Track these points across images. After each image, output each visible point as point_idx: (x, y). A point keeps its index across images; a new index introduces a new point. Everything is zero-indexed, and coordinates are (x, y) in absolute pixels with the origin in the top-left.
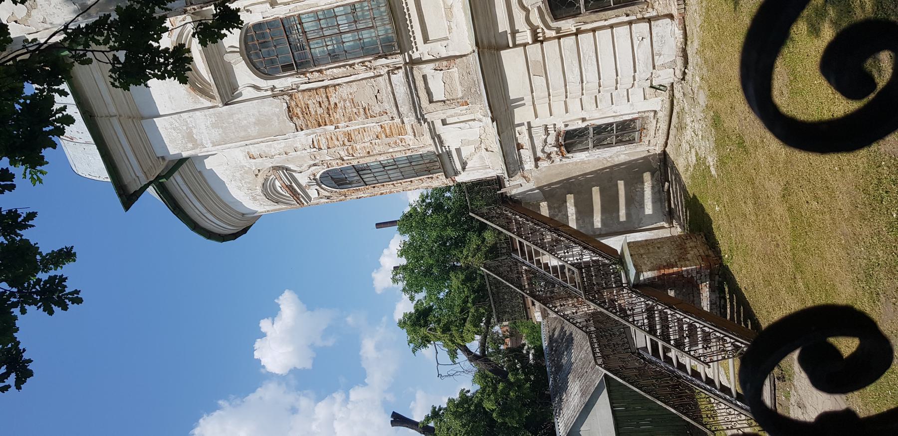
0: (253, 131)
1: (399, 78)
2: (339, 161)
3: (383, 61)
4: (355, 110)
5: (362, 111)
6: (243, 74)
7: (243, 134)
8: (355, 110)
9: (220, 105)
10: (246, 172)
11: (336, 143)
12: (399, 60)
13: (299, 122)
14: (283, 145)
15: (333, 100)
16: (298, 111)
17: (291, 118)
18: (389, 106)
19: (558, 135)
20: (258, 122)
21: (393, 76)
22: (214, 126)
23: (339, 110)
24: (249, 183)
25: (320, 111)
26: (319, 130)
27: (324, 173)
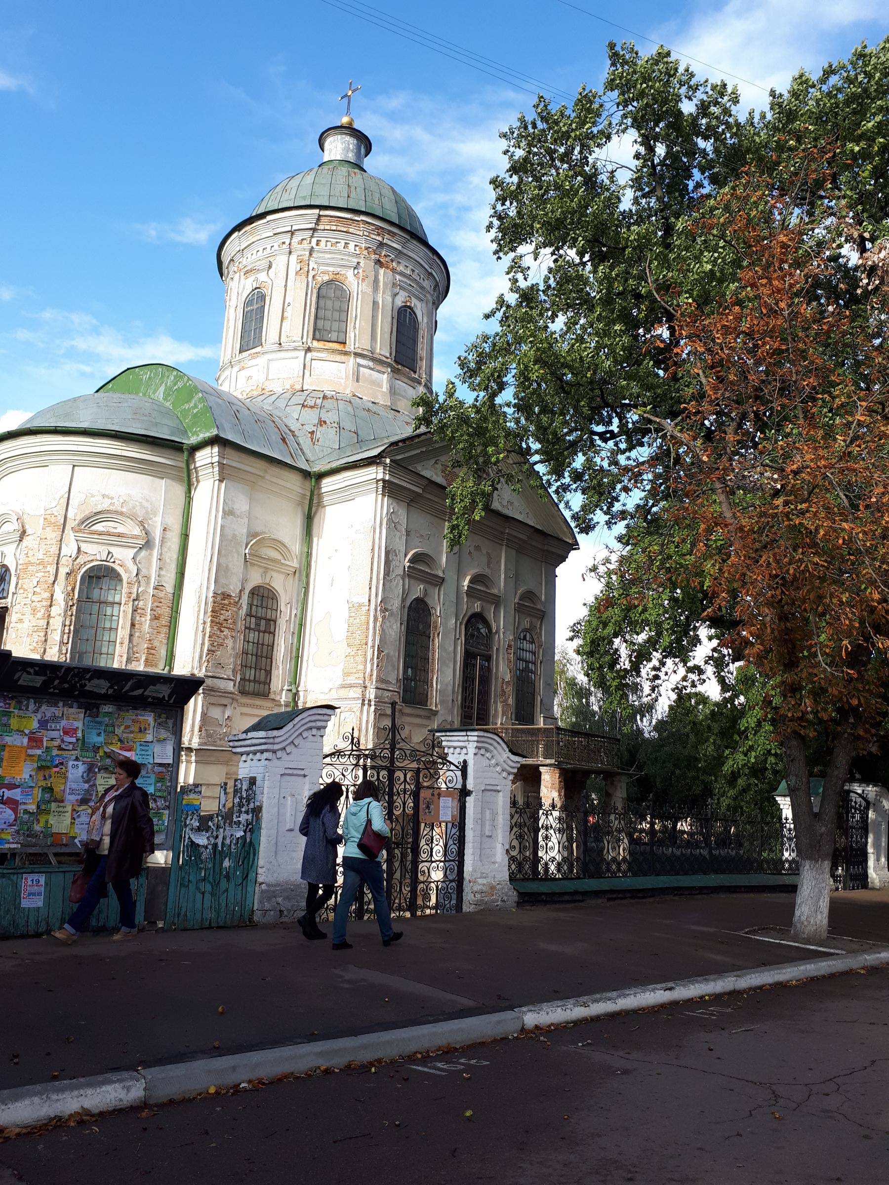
0: (223, 560)
1: (230, 686)
2: (134, 596)
4: (215, 644)
5: (213, 649)
6: (256, 579)
7: (223, 552)
8: (215, 644)
10: (147, 512)
11: (156, 604)
14: (168, 561)
15: (226, 631)
16: (226, 602)
17: (223, 594)
20: (227, 569)
21: (232, 683)
22: (234, 536)
24: (134, 508)
25: (222, 617)
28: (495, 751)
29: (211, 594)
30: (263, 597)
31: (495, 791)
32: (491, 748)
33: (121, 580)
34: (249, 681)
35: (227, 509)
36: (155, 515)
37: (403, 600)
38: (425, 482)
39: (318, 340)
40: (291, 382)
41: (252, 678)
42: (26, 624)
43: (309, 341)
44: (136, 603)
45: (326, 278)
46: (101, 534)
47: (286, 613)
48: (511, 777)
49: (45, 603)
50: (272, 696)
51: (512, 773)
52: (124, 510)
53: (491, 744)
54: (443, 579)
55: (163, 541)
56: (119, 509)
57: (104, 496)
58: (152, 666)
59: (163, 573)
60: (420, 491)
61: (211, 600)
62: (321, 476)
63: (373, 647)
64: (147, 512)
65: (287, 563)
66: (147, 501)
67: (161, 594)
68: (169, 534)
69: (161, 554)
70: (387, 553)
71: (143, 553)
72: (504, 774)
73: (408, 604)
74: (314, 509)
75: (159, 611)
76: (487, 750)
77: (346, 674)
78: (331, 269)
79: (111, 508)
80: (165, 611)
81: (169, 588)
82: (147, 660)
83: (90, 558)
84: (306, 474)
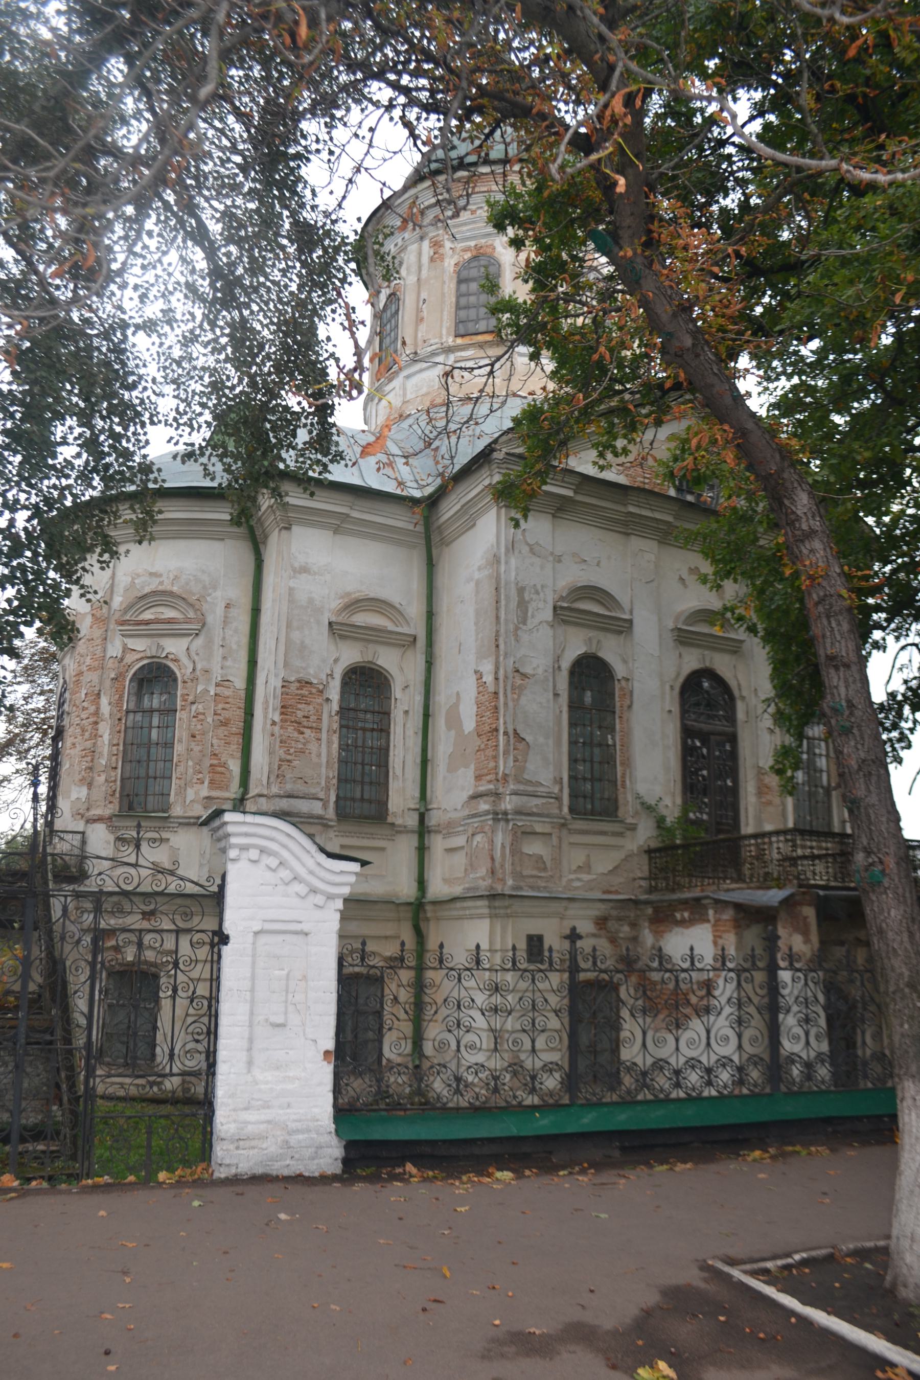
0: (296, 635)
1: (316, 808)
2: (191, 698)
3: (333, 798)
9: (333, 619)
10: (204, 587)
11: (220, 706)
12: (331, 813)
13: (293, 687)
14: (234, 647)
16: (304, 692)
17: (299, 681)
18: (289, 787)
19: (155, 965)
20: (303, 647)
21: (320, 804)
22: (311, 601)
23: (296, 734)
25: (300, 714)
26: (278, 703)
27: (173, 673)
28: (285, 854)
29: (280, 684)
30: (366, 682)
31: (296, 933)
32: (273, 846)
33: (175, 680)
34: (353, 799)
35: (297, 565)
36: (215, 588)
37: (558, 659)
38: (576, 480)
39: (462, 336)
40: (429, 398)
41: (358, 795)
42: (79, 748)
43: (451, 339)
44: (194, 707)
45: (468, 255)
46: (147, 623)
47: (405, 701)
48: (339, 904)
49: (92, 720)
50: (390, 819)
51: (337, 896)
52: (175, 589)
53: (272, 839)
54: (630, 622)
55: (226, 622)
56: (169, 588)
57: (151, 574)
58: (220, 788)
59: (229, 663)
60: (569, 493)
61: (279, 691)
62: (433, 502)
63: (506, 733)
64: (204, 587)
65: (399, 630)
66: (203, 572)
67: (227, 692)
68: (233, 612)
69: (224, 639)
70: (521, 591)
71: (199, 641)
72: (319, 899)
73: (566, 664)
74: (435, 552)
75: (226, 714)
76: (262, 851)
77: (478, 778)
78: (472, 243)
79: (160, 588)
80: (236, 714)
81: (240, 683)
82: (212, 782)
83: (139, 656)
84: (414, 501)
